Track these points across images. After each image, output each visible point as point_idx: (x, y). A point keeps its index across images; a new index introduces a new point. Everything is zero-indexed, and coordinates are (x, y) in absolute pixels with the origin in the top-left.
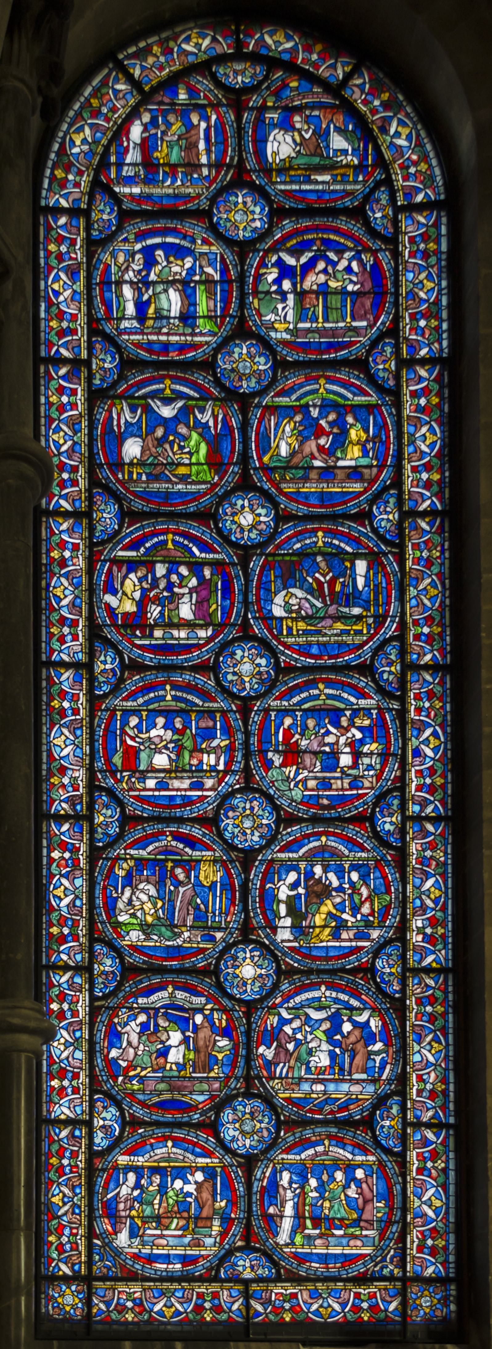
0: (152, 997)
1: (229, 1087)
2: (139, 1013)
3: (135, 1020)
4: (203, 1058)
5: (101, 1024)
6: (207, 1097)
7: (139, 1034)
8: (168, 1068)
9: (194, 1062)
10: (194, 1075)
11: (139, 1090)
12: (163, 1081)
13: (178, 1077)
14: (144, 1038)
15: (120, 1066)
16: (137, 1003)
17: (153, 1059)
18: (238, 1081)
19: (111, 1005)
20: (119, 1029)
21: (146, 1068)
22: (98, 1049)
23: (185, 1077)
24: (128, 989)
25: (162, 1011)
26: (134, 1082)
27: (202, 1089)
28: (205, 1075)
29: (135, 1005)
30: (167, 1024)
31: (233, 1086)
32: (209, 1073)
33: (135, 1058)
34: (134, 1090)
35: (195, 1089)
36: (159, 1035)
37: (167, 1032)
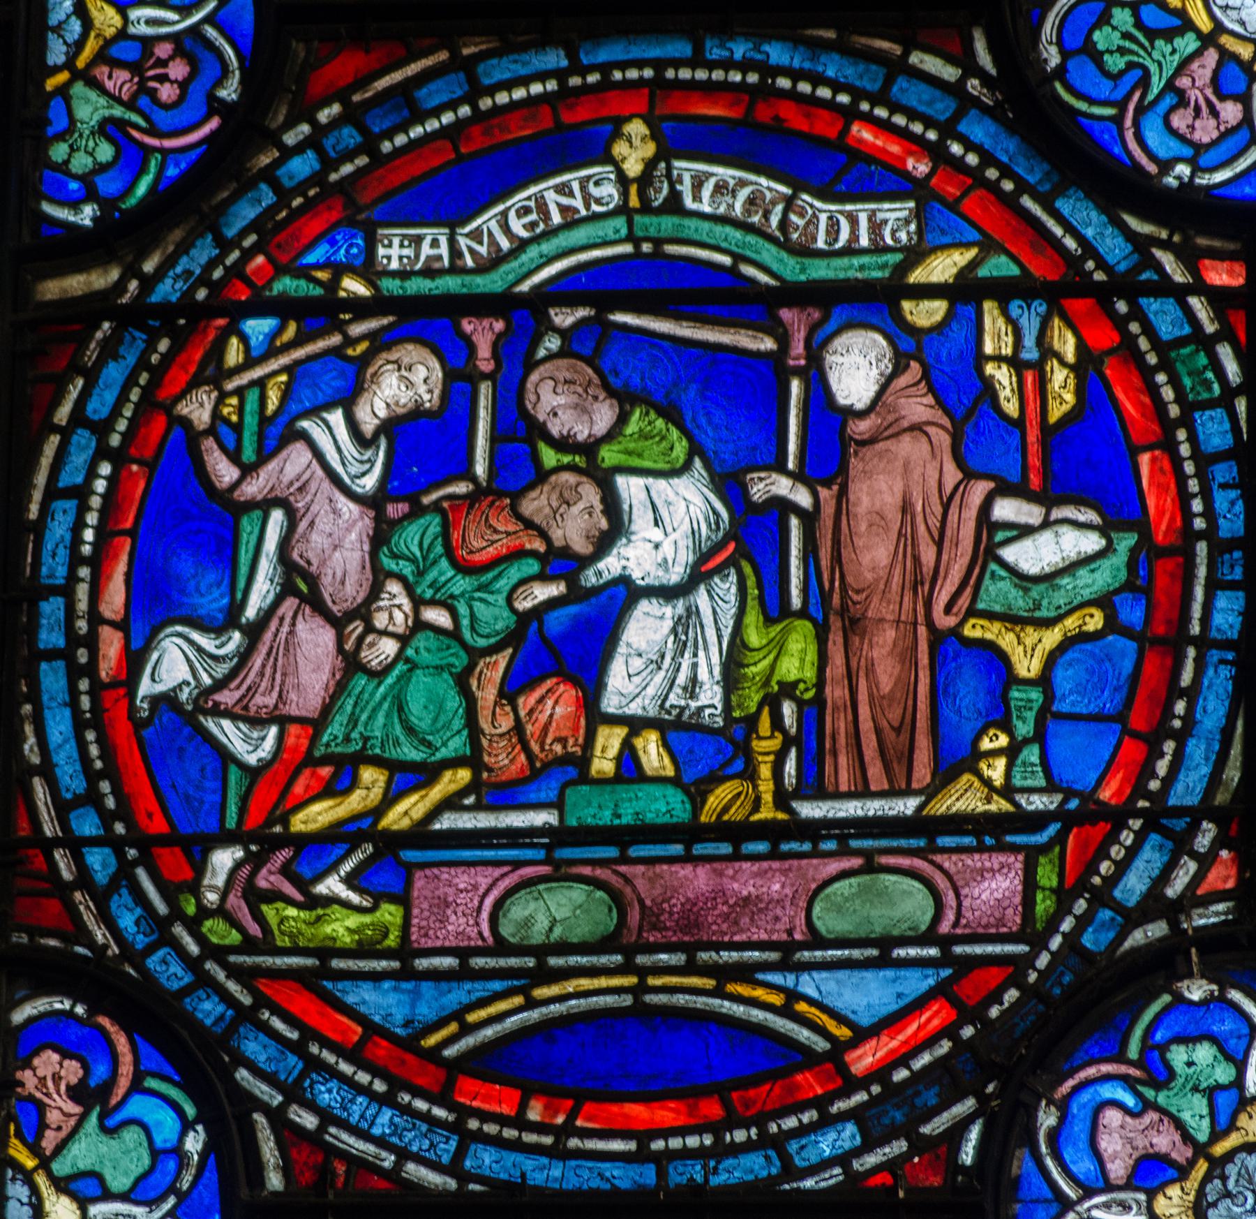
0: (487, 220)
1: (1102, 897)
2: (381, 342)
3: (348, 400)
4: (887, 675)
5: (84, 441)
6: (917, 983)
7: (373, 502)
8: (603, 765)
9: (813, 711)
10: (809, 810)
11: (363, 950)
12: (560, 874)
13: (690, 833)
14: (411, 538)
15: (224, 757)
16: (369, 270)
17: (487, 695)
18: (1181, 845)
19: (167, 290)
20: (224, 472)
21: (424, 775)
22: (51, 637)
23: (736, 833)
24: (303, 166)
25: (564, 318)
26: (332, 885)
27: (881, 919)
28: (907, 806)
29: (353, 286)
30: (604, 416)
31: (1134, 886)
32: (931, 793)
33: (340, 689)
34: (326, 952)
35: (827, 921)
36: (535, 504)
37: (605, 481)
